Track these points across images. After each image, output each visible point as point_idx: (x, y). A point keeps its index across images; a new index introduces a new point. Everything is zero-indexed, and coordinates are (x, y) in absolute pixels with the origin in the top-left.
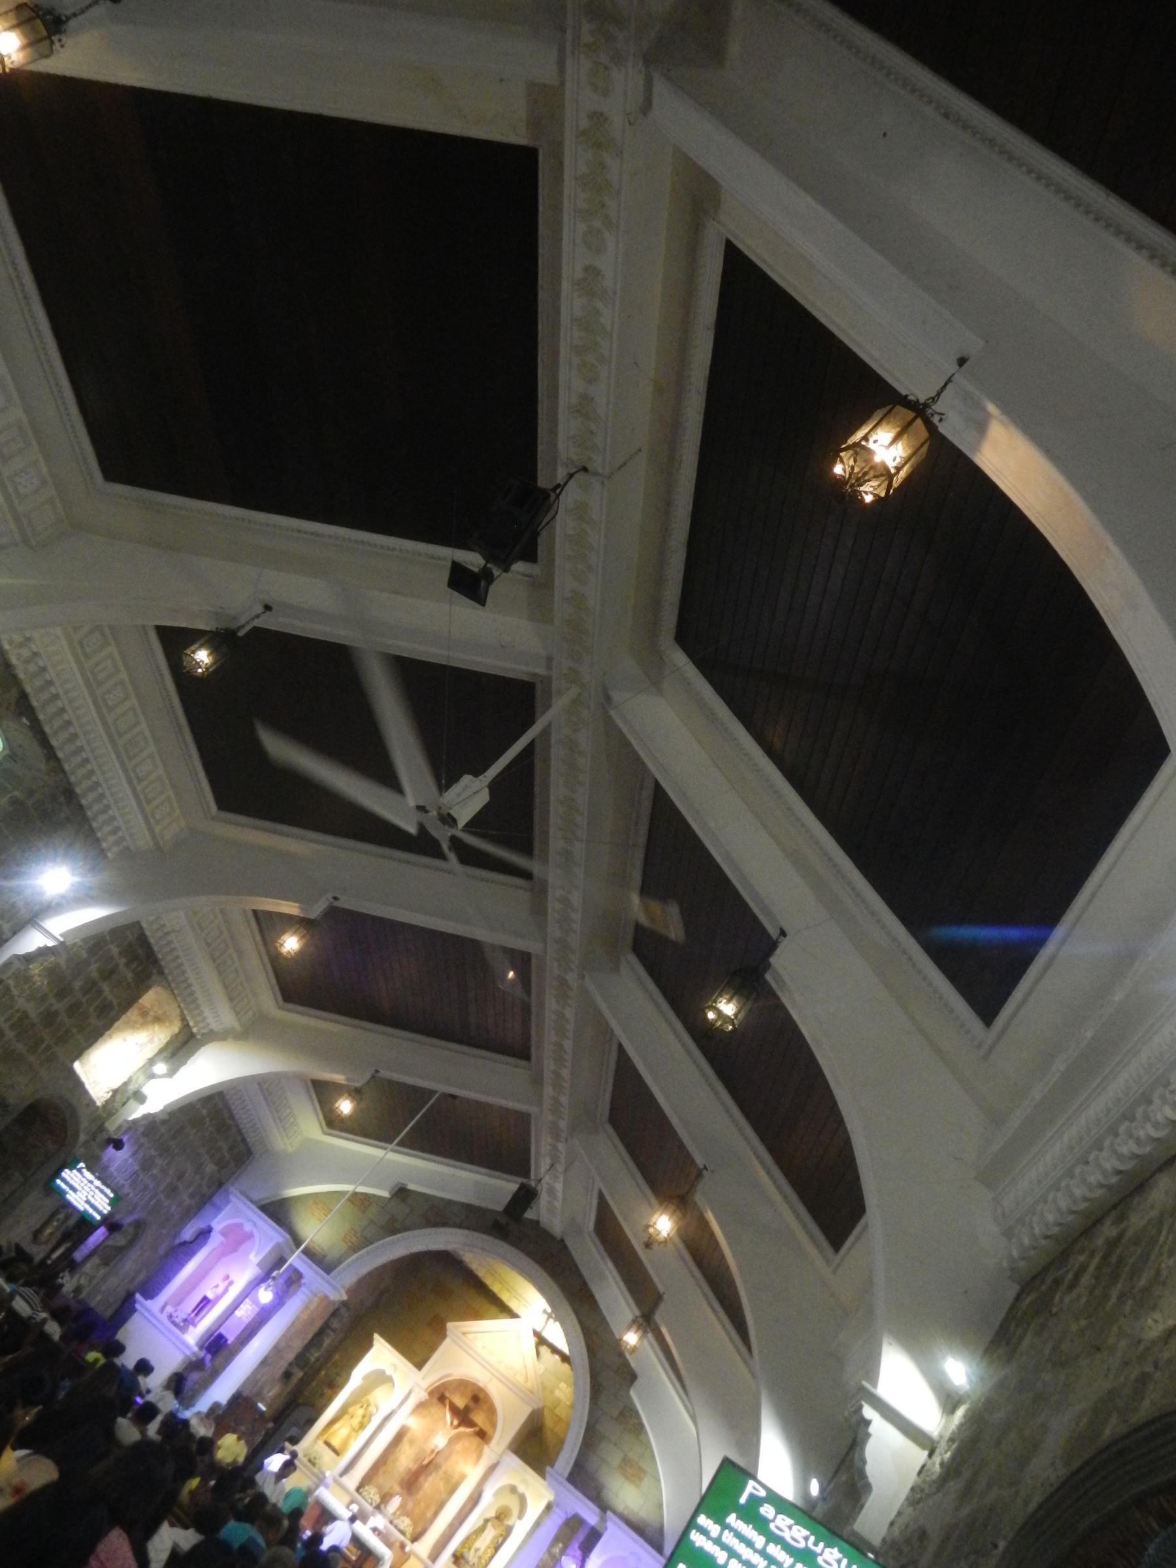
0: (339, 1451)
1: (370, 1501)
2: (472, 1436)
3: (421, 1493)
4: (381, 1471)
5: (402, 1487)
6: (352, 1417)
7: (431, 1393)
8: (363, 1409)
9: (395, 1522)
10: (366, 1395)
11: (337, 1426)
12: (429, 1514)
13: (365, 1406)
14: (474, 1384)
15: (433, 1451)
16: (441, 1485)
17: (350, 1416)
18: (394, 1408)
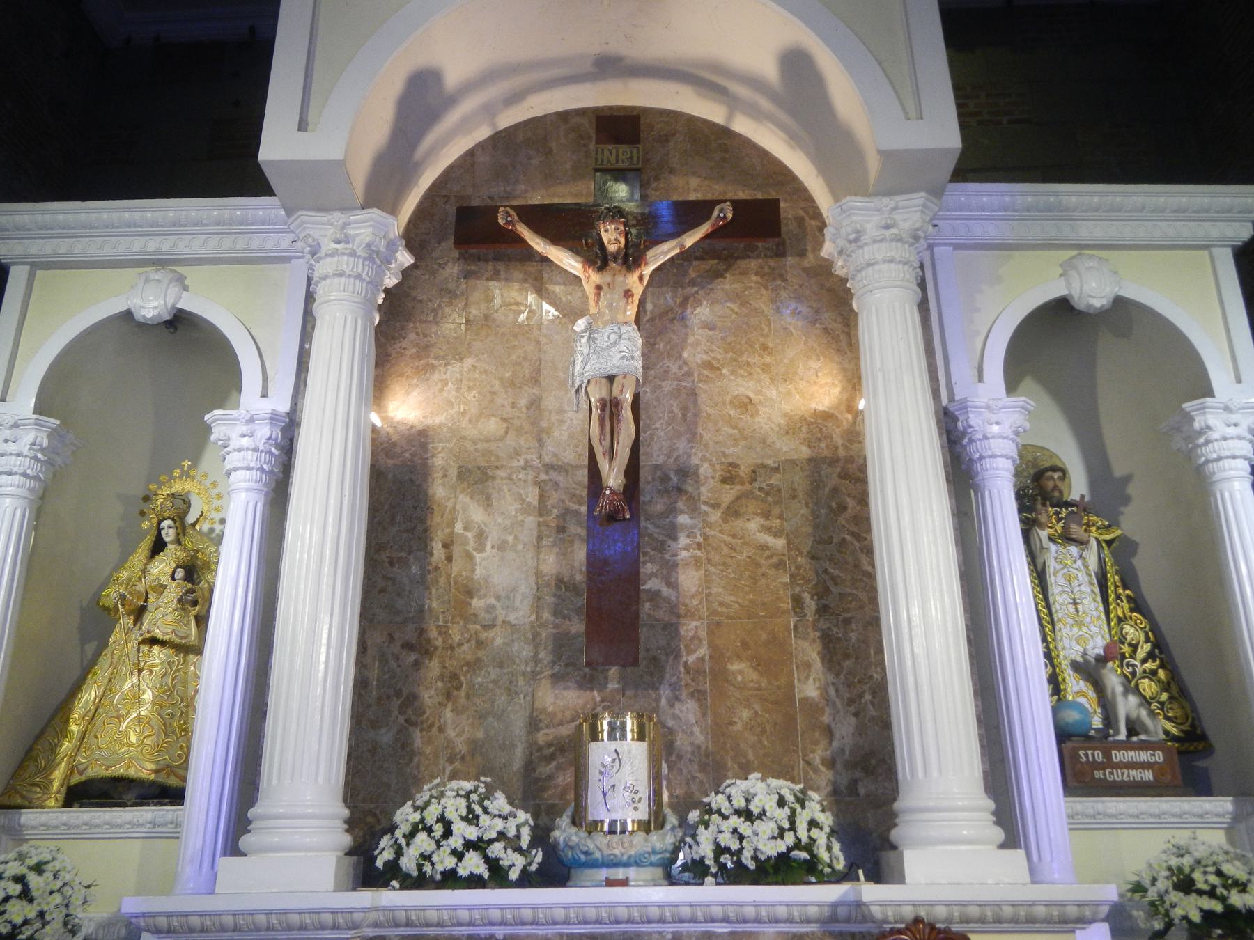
0: (173, 782)
1: (473, 864)
2: (719, 275)
3: (689, 627)
4: (429, 696)
5: (588, 682)
6: (139, 613)
7: (414, 238)
8: (171, 548)
9: (705, 849)
10: (146, 499)
11: (89, 695)
12: (810, 690)
13: (169, 535)
14: (564, 116)
15: (611, 408)
16: (753, 526)
17: (127, 621)
18: (284, 407)
